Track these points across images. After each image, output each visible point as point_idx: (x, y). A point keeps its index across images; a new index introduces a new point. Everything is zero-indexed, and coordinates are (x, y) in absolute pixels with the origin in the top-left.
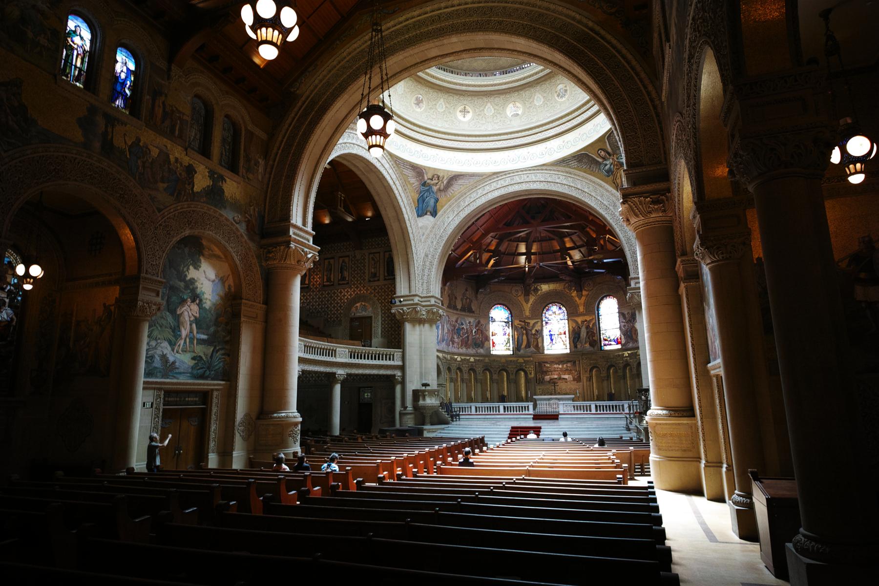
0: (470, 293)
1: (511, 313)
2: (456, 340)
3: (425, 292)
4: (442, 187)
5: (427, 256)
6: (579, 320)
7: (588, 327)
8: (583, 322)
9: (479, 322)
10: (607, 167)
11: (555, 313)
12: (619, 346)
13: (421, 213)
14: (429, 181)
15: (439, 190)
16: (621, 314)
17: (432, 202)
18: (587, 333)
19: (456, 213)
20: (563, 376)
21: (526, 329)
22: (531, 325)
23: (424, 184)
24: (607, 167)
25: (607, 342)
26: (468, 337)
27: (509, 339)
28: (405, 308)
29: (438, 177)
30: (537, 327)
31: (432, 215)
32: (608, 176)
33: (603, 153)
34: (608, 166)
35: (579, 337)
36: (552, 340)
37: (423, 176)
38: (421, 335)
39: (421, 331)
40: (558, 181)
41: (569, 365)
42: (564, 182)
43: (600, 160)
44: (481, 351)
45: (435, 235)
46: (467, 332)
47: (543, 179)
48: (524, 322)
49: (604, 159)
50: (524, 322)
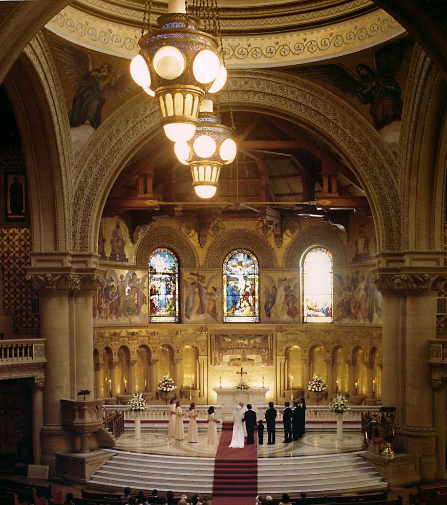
0: (124, 231)
1: (178, 261)
2: (104, 306)
3: (78, 247)
5: (81, 189)
6: (276, 276)
7: (287, 289)
8: (281, 281)
9: (134, 274)
10: (365, 91)
11: (240, 263)
12: (329, 320)
16: (338, 279)
17: (95, 104)
18: (286, 296)
19: (130, 125)
20: (249, 356)
21: (199, 286)
22: (207, 280)
23: (87, 77)
25: (312, 312)
26: (119, 299)
27: (174, 299)
28: (49, 275)
30: (215, 283)
32: (365, 103)
34: (368, 90)
35: (274, 302)
36: (235, 303)
38: (71, 315)
39: (71, 309)
40: (291, 97)
41: (258, 340)
42: (301, 100)
44: (136, 319)
45: (97, 157)
46: (118, 293)
47: (268, 91)
48: (197, 275)
50: (197, 275)
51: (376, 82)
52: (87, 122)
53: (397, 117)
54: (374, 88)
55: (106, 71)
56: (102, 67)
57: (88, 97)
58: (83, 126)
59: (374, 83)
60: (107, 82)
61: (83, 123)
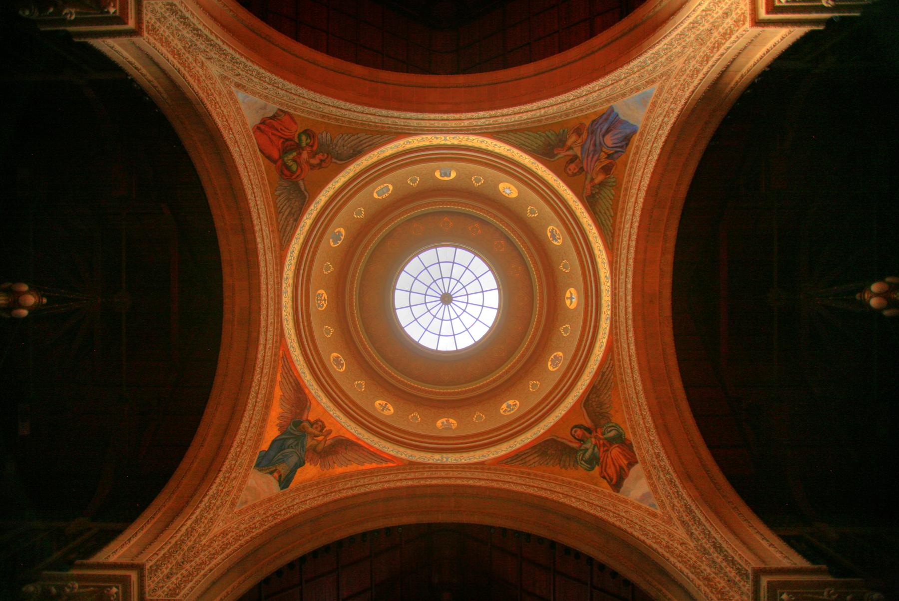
4: (320, 447)
5: (224, 533)
13: (265, 463)
14: (306, 424)
15: (314, 449)
19: (323, 492)
23: (297, 424)
24: (587, 455)
29: (323, 427)
31: (279, 481)
32: (592, 468)
33: (579, 432)
37: (303, 411)
43: (575, 445)
49: (581, 441)
51: (596, 437)
52: (276, 474)
53: (632, 463)
54: (596, 445)
55: (319, 429)
56: (317, 421)
57: (288, 447)
58: (269, 476)
59: (593, 440)
60: (315, 442)
61: (271, 473)
